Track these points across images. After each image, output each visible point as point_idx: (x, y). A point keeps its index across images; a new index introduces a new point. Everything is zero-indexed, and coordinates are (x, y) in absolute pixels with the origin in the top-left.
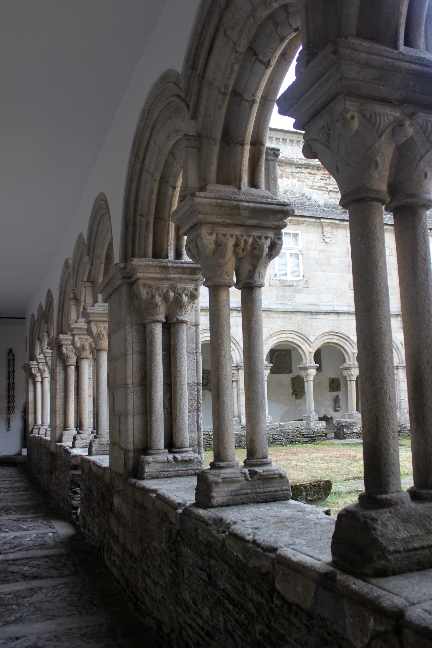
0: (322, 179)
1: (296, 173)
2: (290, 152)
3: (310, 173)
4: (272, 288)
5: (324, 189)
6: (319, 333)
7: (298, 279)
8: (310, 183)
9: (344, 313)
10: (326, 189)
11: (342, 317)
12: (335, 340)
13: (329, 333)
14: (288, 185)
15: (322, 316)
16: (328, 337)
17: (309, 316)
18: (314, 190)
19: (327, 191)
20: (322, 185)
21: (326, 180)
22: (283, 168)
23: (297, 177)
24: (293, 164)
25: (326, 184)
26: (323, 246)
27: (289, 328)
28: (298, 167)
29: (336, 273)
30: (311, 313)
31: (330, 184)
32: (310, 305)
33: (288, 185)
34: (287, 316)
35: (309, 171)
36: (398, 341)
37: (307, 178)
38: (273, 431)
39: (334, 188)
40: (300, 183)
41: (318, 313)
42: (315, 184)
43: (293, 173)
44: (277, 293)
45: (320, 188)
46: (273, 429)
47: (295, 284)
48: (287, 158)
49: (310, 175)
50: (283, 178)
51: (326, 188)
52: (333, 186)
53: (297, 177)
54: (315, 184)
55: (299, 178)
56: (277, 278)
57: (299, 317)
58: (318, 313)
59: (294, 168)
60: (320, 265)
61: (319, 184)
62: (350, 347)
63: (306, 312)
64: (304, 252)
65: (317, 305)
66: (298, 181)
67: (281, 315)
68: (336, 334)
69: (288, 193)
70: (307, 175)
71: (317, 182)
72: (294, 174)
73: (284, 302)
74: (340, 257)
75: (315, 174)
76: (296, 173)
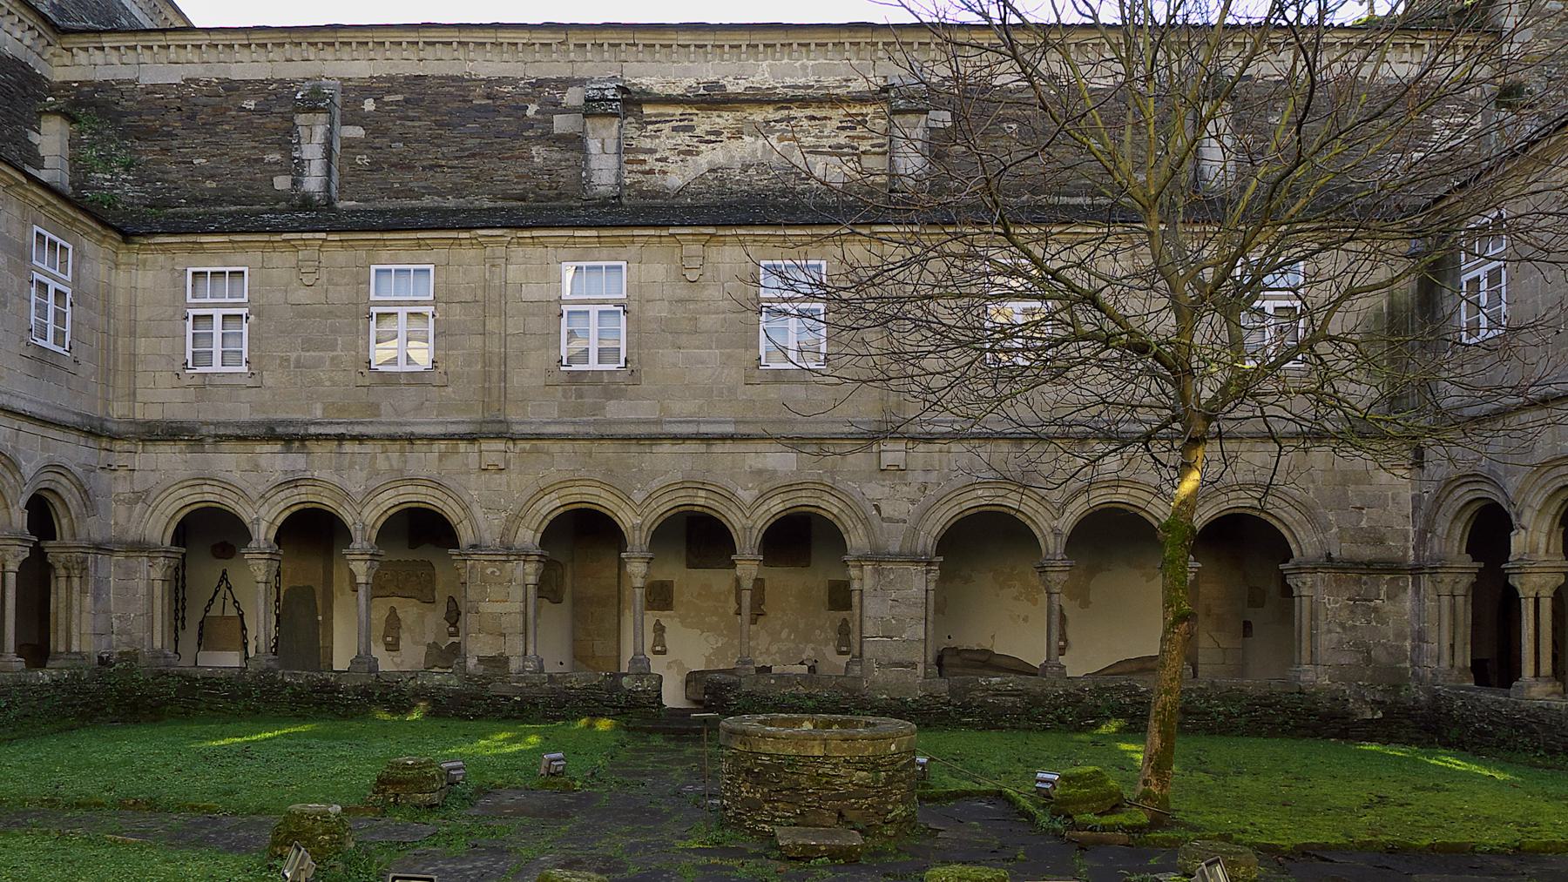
0: (843, 128)
1: (775, 121)
2: (767, 75)
3: (813, 118)
4: (551, 389)
5: (845, 150)
6: (655, 484)
7: (613, 367)
8: (810, 141)
9: (723, 438)
10: (851, 151)
11: (718, 448)
12: (701, 499)
13: (683, 485)
14: (754, 151)
15: (666, 448)
16: (682, 493)
17: (634, 448)
18: (819, 158)
19: (854, 154)
20: (842, 140)
21: (851, 128)
22: (744, 115)
23: (778, 131)
24: (769, 102)
25: (853, 138)
26: (682, 291)
27: (583, 473)
28: (782, 108)
29: (711, 348)
30: (638, 439)
31: (864, 138)
32: (639, 422)
33: (754, 151)
34: (581, 446)
35: (809, 112)
36: (867, 502)
37: (804, 131)
38: (535, 690)
39: (873, 146)
40: (786, 143)
41: (655, 439)
42: (824, 142)
43: (768, 122)
44: (563, 400)
45: (836, 151)
46: (535, 685)
47: (606, 379)
48: (759, 89)
49: (813, 123)
50: (744, 137)
51: (853, 148)
52: (870, 142)
53: (778, 131)
54: (824, 142)
55: (784, 131)
56: (562, 368)
57: (609, 449)
58: (655, 439)
59: (771, 111)
60: (671, 333)
61: (834, 141)
62: (740, 515)
63: (627, 438)
64: (634, 307)
65: (658, 422)
66: (780, 140)
67: (568, 446)
68: (702, 485)
69: (751, 171)
70: (805, 123)
71: (829, 137)
72: (772, 124)
73: (577, 419)
74: (724, 313)
75: (825, 118)
76: (775, 121)
